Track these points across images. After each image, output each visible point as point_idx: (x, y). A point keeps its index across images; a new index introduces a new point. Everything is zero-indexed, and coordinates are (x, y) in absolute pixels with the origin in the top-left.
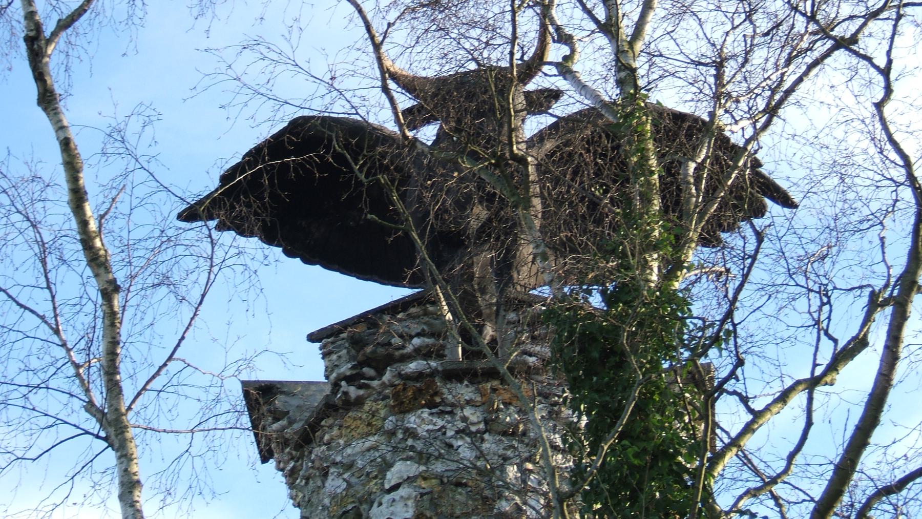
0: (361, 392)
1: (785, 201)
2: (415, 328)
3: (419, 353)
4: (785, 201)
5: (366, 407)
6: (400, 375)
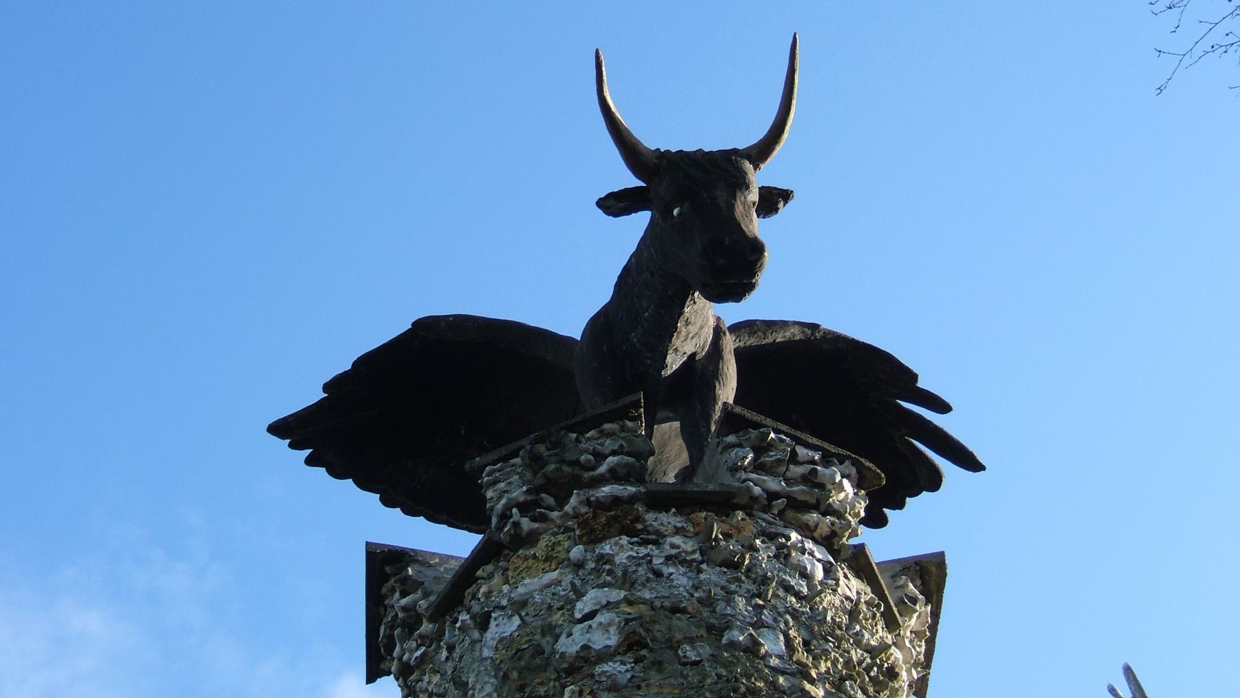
0: (536, 525)
1: (969, 462)
2: (610, 445)
3: (614, 476)
4: (969, 462)
5: (542, 543)
6: (588, 502)
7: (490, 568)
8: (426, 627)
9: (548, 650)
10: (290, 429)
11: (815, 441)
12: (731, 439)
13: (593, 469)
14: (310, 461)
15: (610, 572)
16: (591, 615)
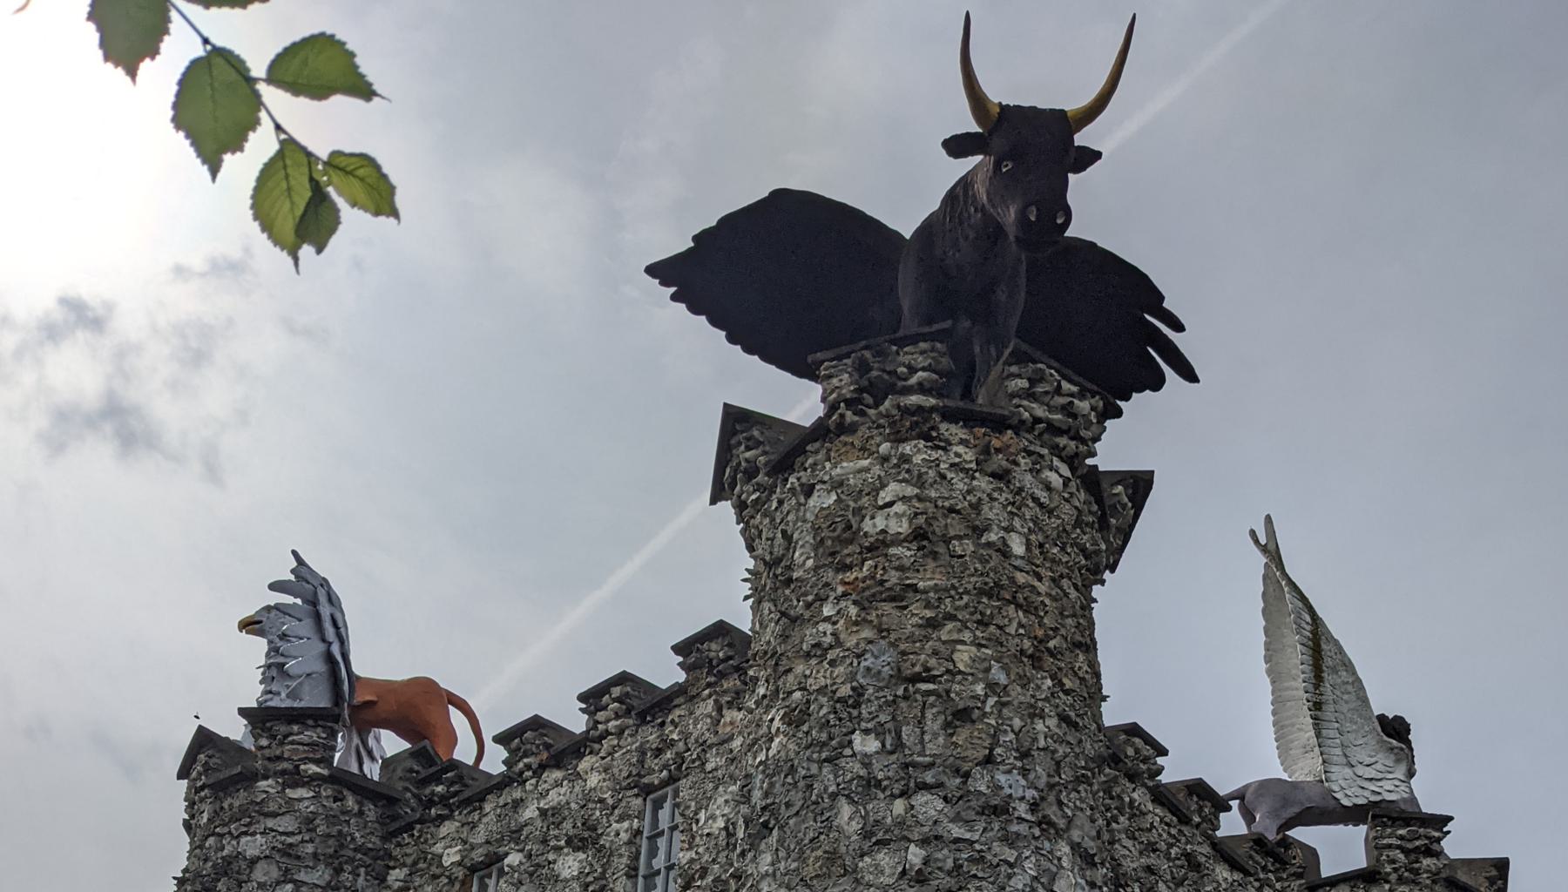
0: (856, 418)
1: (1189, 375)
3: (921, 388)
4: (1189, 375)
5: (860, 433)
6: (899, 407)
7: (817, 445)
8: (761, 478)
9: (855, 526)
10: (661, 271)
11: (1076, 378)
12: (1014, 369)
13: (905, 380)
14: (674, 298)
15: (908, 471)
16: (890, 504)
